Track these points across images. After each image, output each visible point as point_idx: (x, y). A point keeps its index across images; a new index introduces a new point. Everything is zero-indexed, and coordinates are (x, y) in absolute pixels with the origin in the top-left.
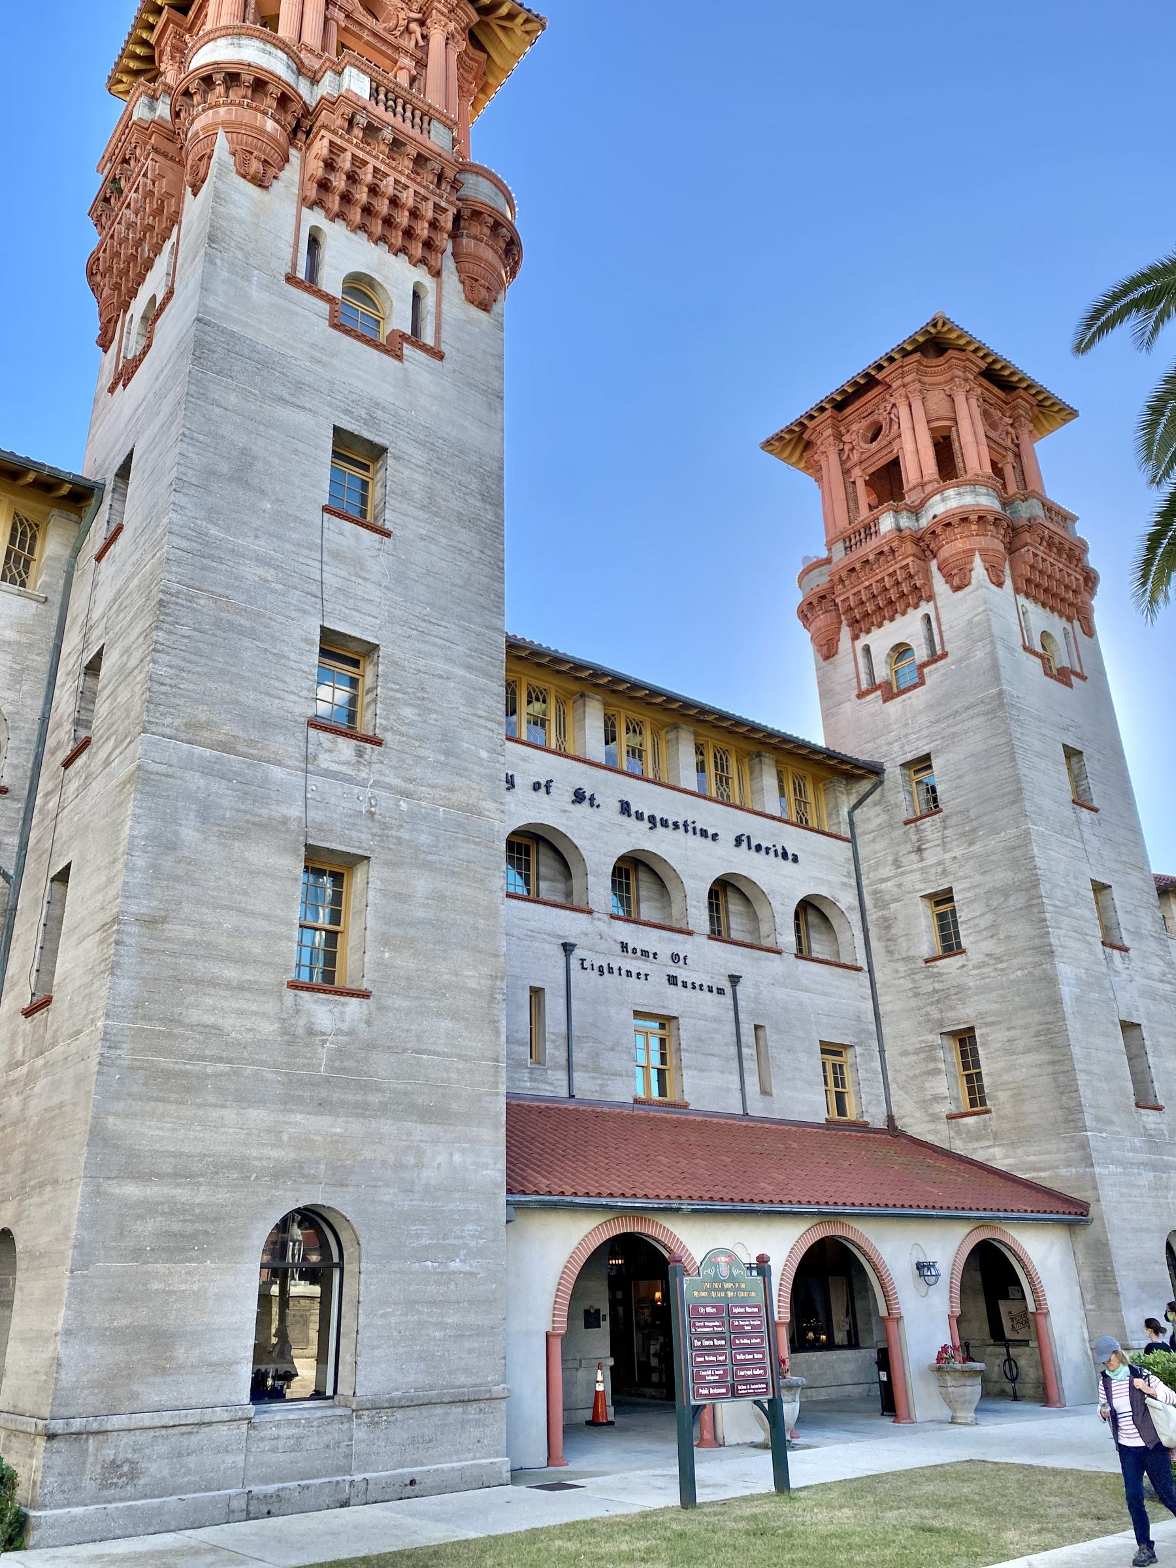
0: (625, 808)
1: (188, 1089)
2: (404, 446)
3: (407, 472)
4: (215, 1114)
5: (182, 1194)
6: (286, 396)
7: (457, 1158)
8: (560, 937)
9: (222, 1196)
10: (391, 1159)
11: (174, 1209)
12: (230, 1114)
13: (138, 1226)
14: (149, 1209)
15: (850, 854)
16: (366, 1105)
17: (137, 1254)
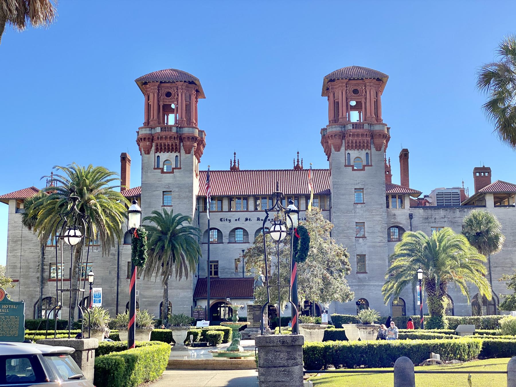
0: (258, 219)
1: (150, 288)
2: (174, 189)
3: (175, 194)
4: (153, 291)
5: (150, 300)
6: (155, 190)
7: (185, 294)
8: (242, 249)
9: (154, 300)
10: (175, 294)
11: (149, 301)
12: (155, 291)
13: (146, 303)
14: (146, 301)
15: (329, 214)
16: (172, 288)
17: (146, 306)
